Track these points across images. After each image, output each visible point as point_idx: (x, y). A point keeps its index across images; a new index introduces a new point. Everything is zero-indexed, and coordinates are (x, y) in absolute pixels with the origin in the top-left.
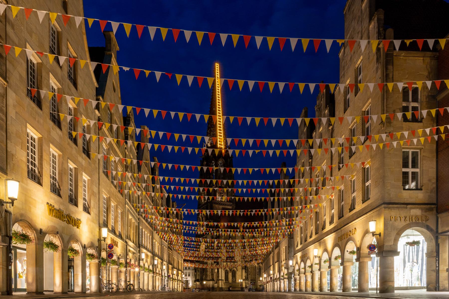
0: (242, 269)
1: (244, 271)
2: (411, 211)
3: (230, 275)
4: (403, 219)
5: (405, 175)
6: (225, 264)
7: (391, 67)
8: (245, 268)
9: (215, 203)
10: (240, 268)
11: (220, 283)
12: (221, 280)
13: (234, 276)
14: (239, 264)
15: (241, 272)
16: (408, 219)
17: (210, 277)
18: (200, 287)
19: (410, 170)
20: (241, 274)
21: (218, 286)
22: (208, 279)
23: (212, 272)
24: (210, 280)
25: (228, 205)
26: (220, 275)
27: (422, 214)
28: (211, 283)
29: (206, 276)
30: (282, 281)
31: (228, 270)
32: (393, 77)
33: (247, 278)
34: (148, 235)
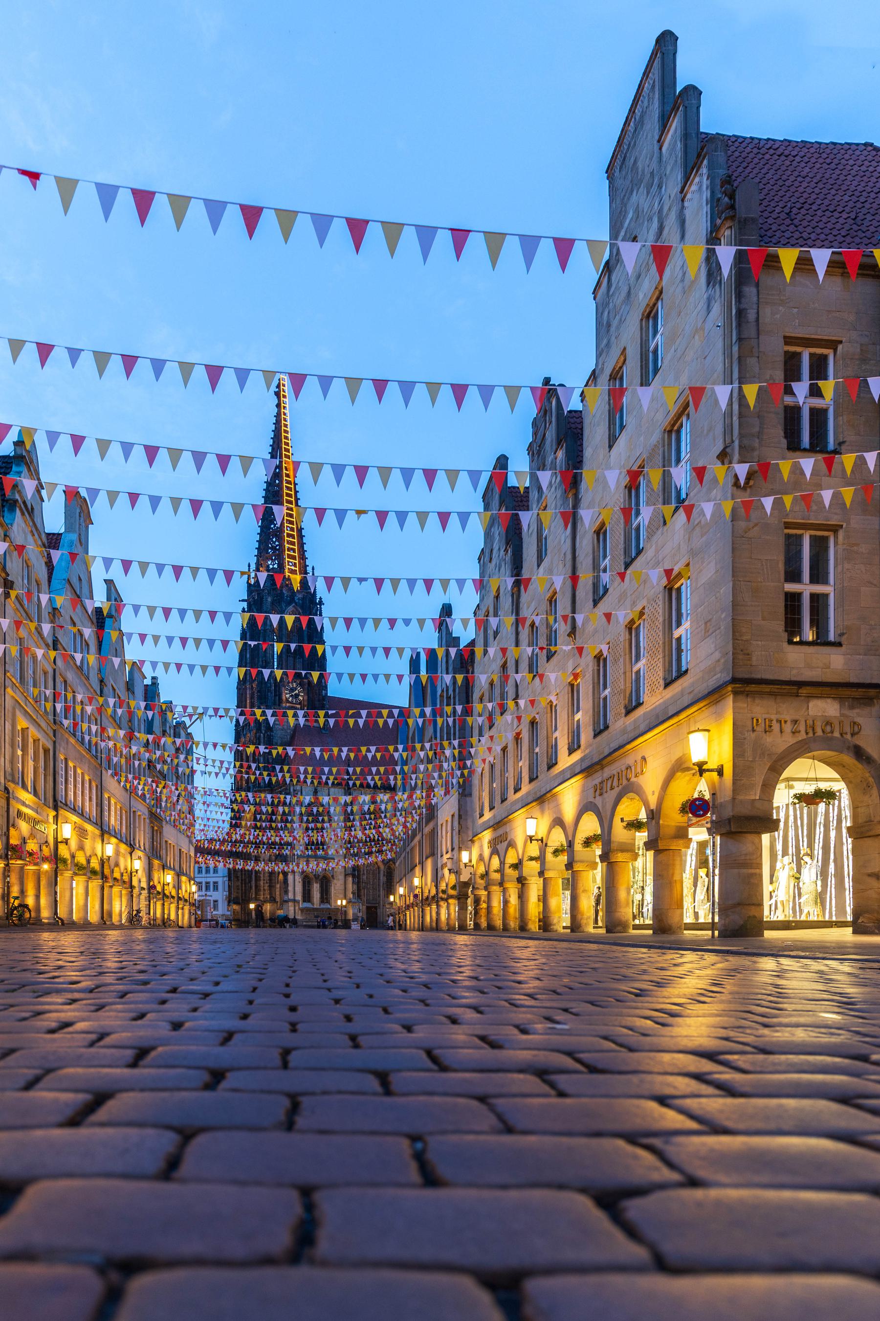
1: (350, 879)
2: (811, 704)
3: (316, 888)
4: (788, 728)
5: (793, 601)
7: (753, 290)
15: (342, 881)
16: (802, 728)
19: (806, 588)
23: (270, 880)
26: (290, 888)
27: (842, 715)
30: (443, 905)
32: (757, 320)
34: (87, 778)
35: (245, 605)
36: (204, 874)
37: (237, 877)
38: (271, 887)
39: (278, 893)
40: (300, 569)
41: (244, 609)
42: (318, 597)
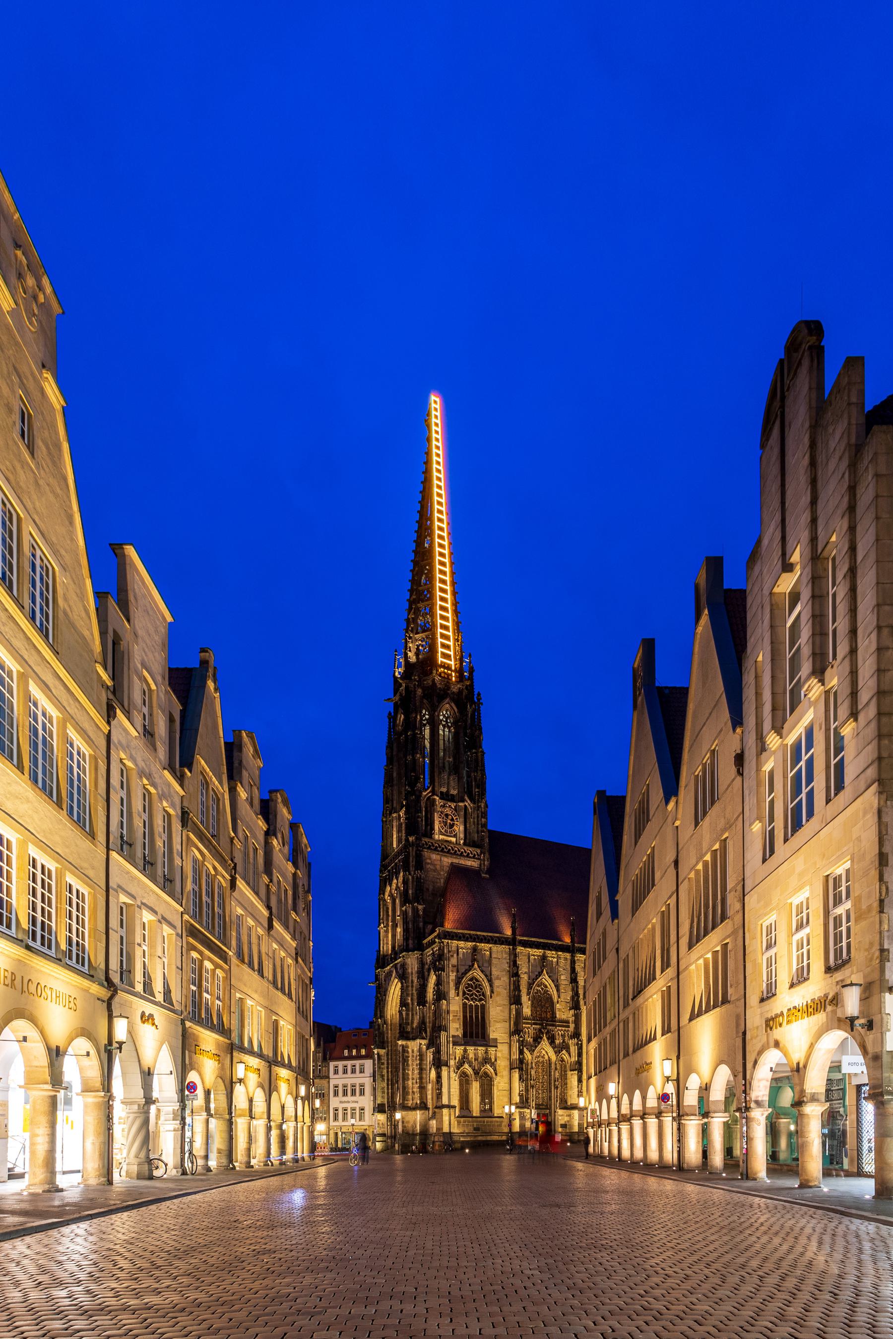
0: (511, 1069)
6: (459, 1050)
8: (520, 1065)
9: (429, 848)
10: (503, 1064)
11: (446, 1119)
12: (449, 1107)
13: (487, 1093)
14: (502, 1053)
17: (414, 1098)
18: (387, 1130)
20: (507, 1087)
21: (439, 1129)
22: (410, 1103)
23: (421, 1078)
24: (414, 1108)
25: (468, 856)
26: (445, 1090)
28: (417, 1117)
29: (405, 1093)
33: (527, 1099)
36: (349, 1074)
37: (382, 1076)
38: (422, 1088)
40: (455, 653)
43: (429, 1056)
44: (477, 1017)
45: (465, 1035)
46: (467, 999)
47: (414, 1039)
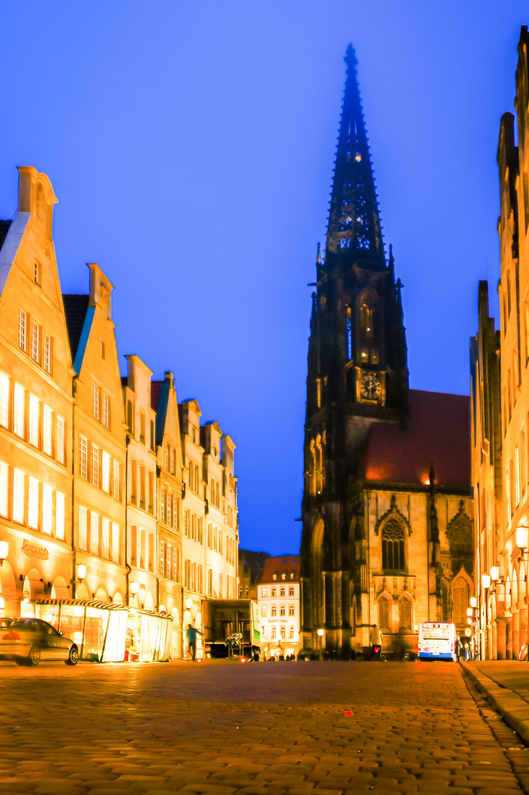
1: (434, 600)
6: (378, 580)
12: (368, 626)
24: (337, 628)
31: (389, 596)
35: (314, 289)
39: (352, 618)
41: (314, 293)
42: (396, 278)
43: (351, 585)
44: (396, 552)
45: (384, 566)
46: (387, 537)
47: (337, 570)
